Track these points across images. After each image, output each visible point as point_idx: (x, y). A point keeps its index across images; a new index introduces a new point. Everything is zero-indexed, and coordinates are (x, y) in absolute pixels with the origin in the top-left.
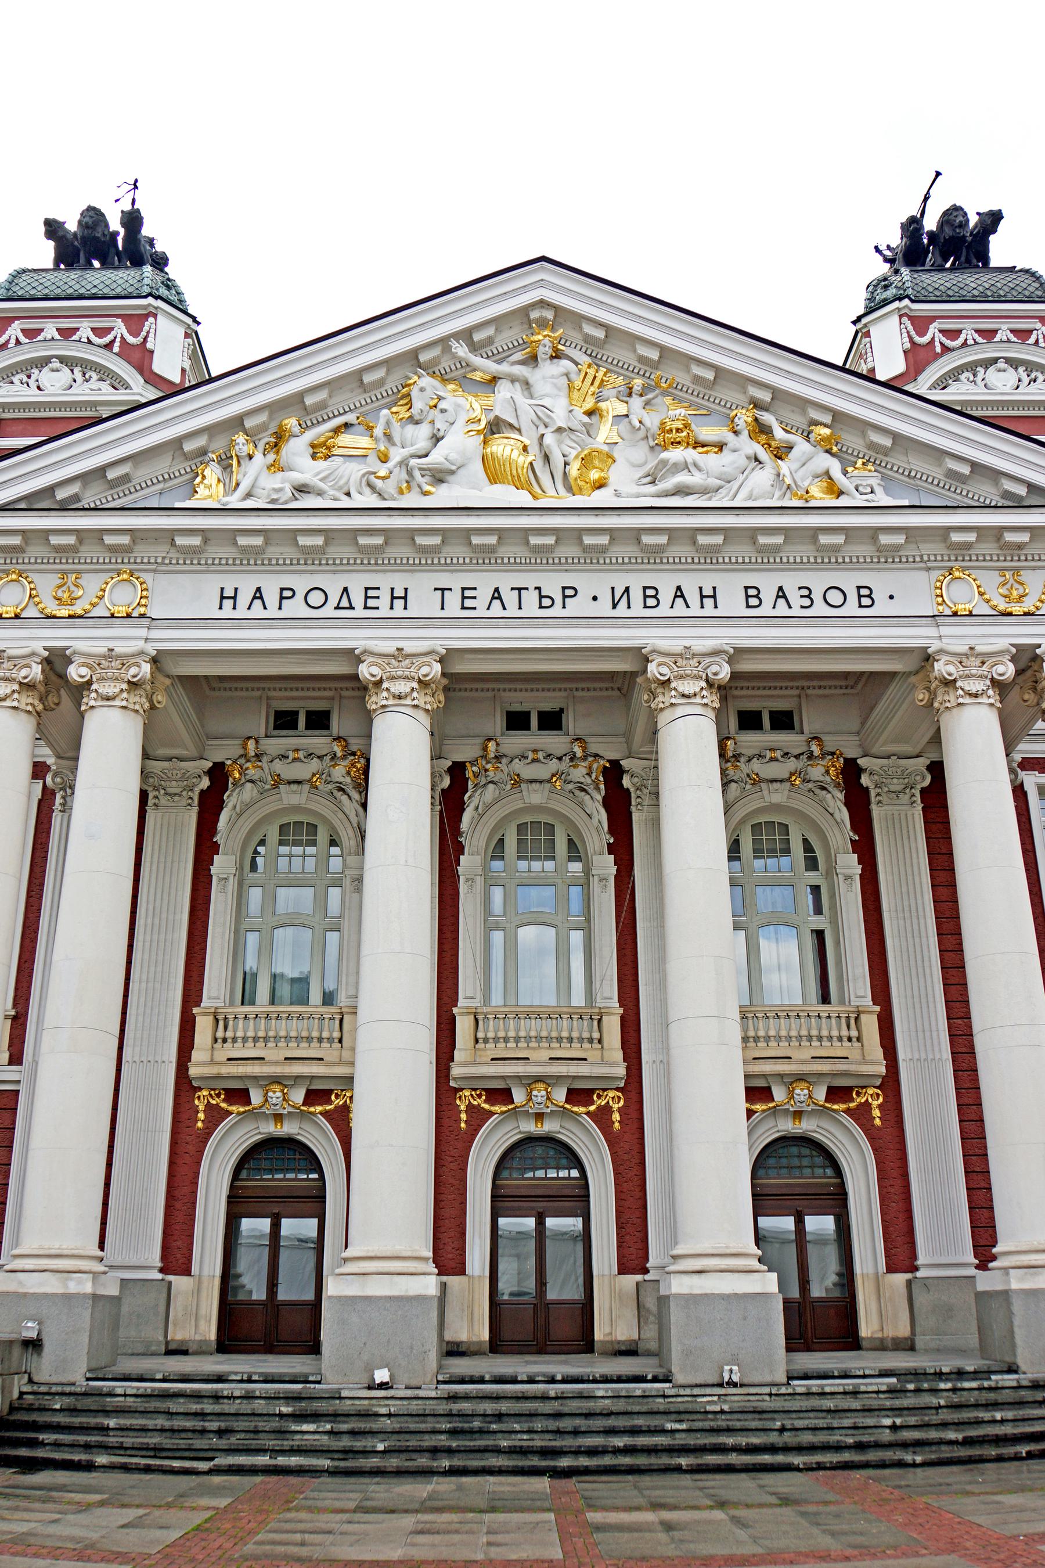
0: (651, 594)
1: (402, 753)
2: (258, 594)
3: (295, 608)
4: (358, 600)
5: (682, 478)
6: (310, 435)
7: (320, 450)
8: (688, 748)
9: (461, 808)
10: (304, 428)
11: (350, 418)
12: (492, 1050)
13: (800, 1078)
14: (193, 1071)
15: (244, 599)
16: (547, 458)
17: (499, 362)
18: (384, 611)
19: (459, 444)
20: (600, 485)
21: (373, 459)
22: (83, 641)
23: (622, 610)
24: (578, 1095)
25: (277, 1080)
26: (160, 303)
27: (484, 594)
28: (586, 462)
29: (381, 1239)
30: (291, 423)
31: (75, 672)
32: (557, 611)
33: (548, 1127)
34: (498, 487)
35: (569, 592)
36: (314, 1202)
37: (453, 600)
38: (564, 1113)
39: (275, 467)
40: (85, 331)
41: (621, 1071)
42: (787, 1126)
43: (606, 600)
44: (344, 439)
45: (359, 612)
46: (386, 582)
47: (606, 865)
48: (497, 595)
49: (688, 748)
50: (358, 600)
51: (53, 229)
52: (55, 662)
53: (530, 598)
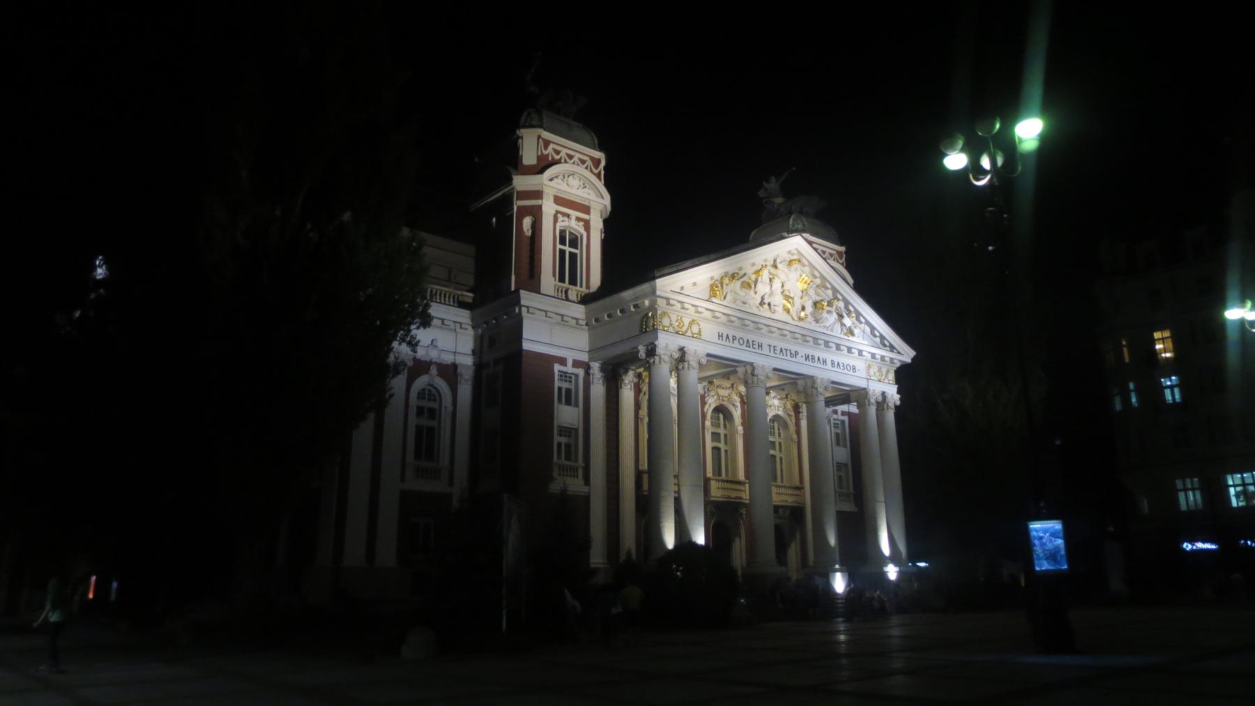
0: (813, 358)
3: (736, 344)
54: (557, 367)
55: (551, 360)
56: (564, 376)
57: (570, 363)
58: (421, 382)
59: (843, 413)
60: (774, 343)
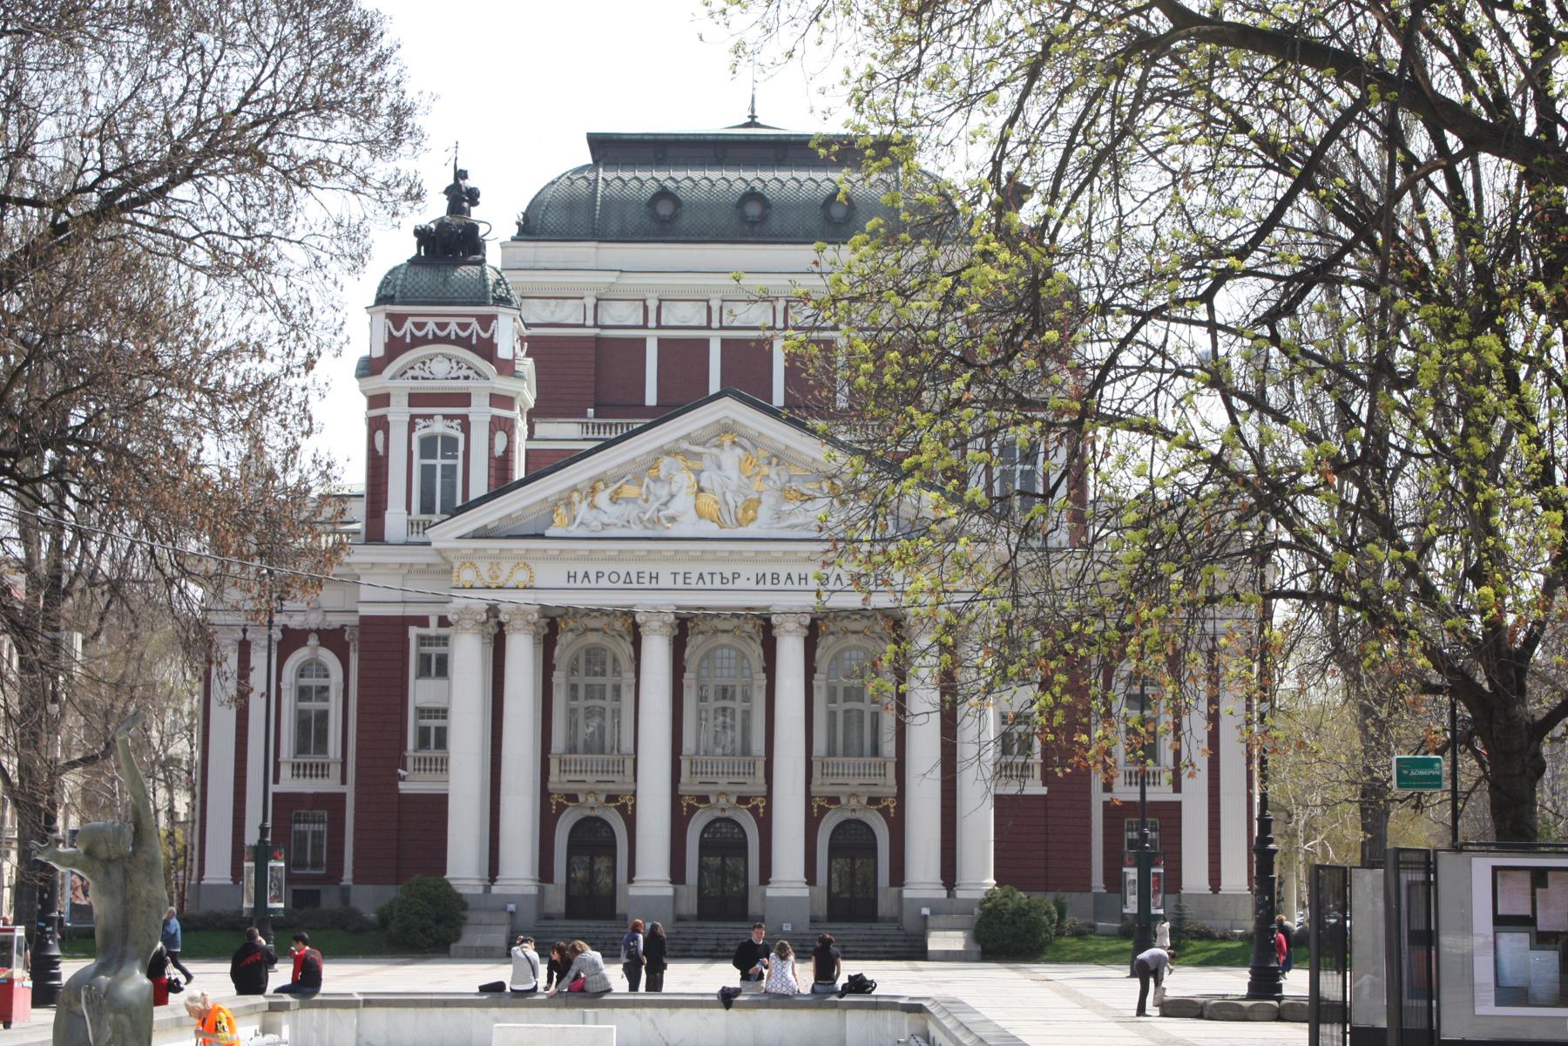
0: (775, 577)
1: (657, 652)
2: (586, 575)
3: (604, 582)
4: (634, 579)
5: (793, 521)
6: (609, 491)
7: (614, 499)
8: (790, 652)
9: (684, 646)
10: (606, 486)
11: (629, 477)
12: (699, 778)
13: (853, 795)
14: (550, 786)
15: (580, 576)
16: (727, 504)
17: (704, 444)
18: (647, 585)
20: (753, 520)
21: (640, 502)
23: (761, 586)
24: (743, 800)
25: (592, 792)
26: (501, 309)
27: (695, 576)
28: (745, 511)
29: (651, 874)
30: (601, 485)
31: (503, 618)
32: (730, 586)
33: (727, 814)
34: (702, 522)
35: (736, 576)
36: (610, 848)
37: (680, 579)
38: (735, 808)
39: (593, 506)
40: (453, 327)
41: (763, 788)
42: (848, 815)
43: (754, 580)
44: (626, 487)
45: (635, 585)
46: (648, 568)
47: (761, 679)
48: (701, 576)
49: (790, 652)
50: (634, 579)
51: (417, 233)
52: (493, 610)
53: (717, 578)
54: (414, 632)
55: (406, 621)
56: (423, 640)
57: (433, 621)
58: (299, 656)
60: (681, 569)
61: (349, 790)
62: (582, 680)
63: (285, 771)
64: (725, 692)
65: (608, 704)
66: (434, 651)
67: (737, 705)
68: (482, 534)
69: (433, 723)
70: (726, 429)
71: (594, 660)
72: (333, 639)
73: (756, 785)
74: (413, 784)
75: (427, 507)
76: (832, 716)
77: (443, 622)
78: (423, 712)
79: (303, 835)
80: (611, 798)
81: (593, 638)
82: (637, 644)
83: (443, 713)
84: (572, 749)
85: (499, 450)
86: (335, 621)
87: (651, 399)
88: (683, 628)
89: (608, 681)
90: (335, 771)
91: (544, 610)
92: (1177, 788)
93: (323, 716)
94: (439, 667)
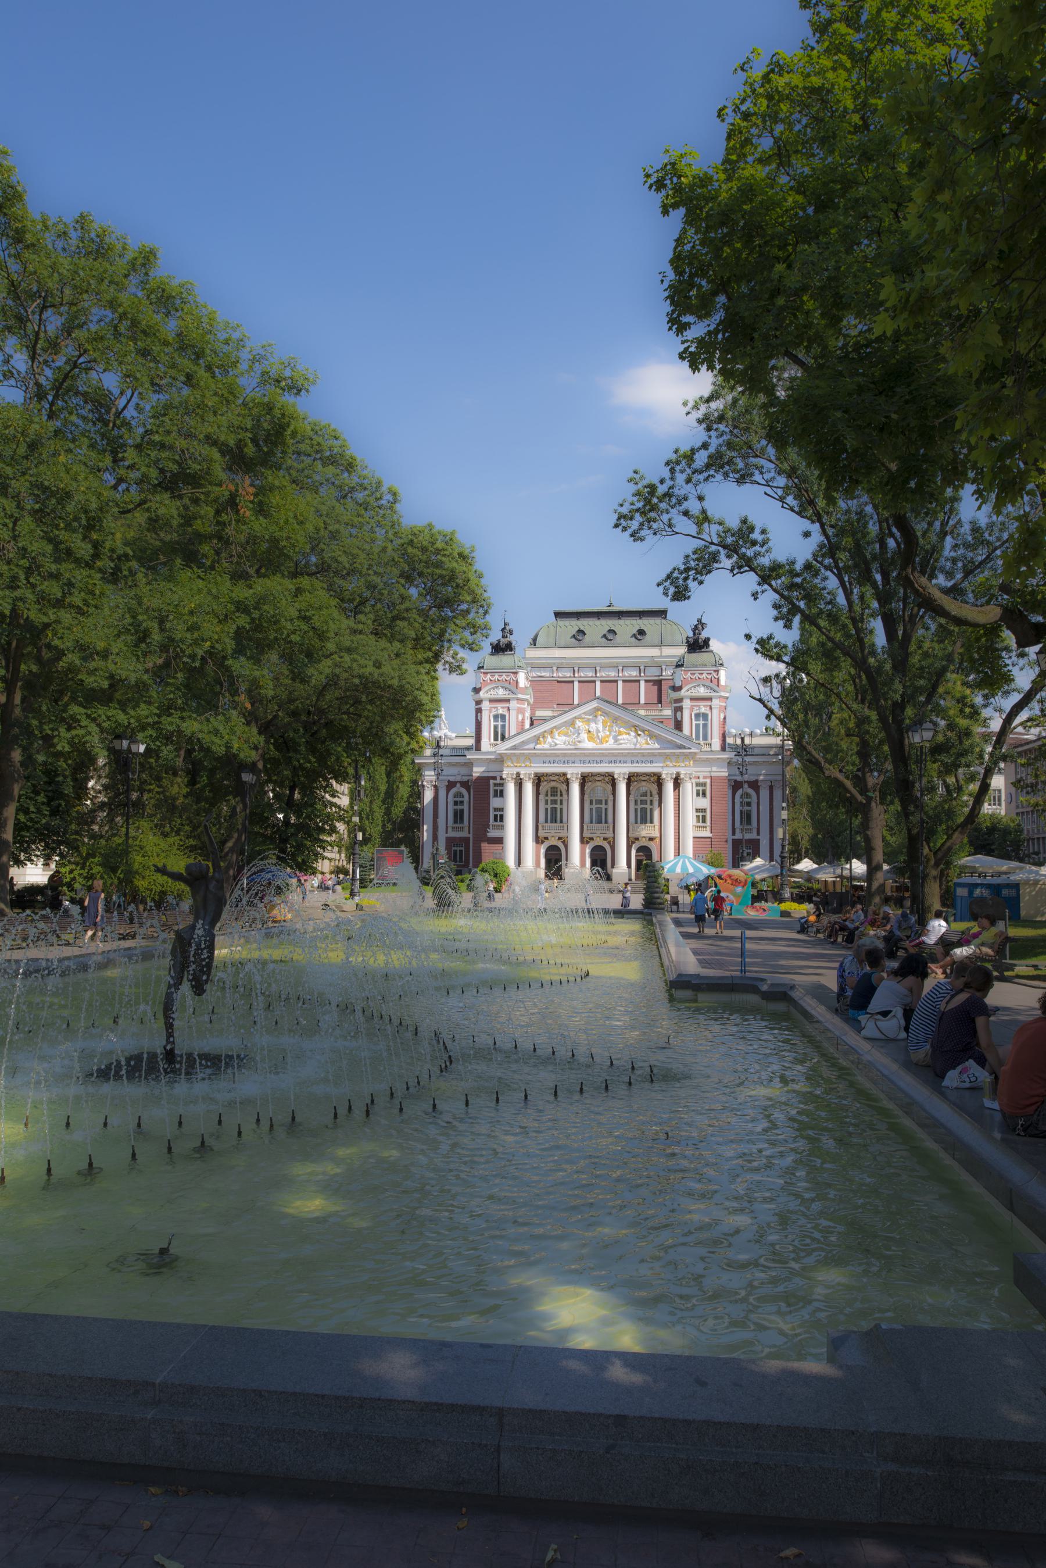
8: (622, 788)
19: (584, 736)
22: (523, 772)
24: (605, 839)
47: (611, 797)
49: (622, 788)
52: (518, 774)
54: (492, 782)
56: (495, 785)
58: (454, 791)
59: (705, 777)
61: (471, 836)
62: (549, 798)
63: (450, 829)
64: (599, 802)
65: (558, 806)
66: (499, 788)
67: (603, 806)
68: (514, 748)
69: (499, 813)
70: (597, 709)
71: (554, 791)
72: (465, 784)
73: (609, 834)
74: (492, 833)
75: (496, 739)
76: (636, 810)
77: (502, 778)
78: (496, 809)
79: (455, 852)
80: (560, 839)
81: (553, 784)
82: (568, 785)
83: (502, 810)
84: (546, 822)
85: (520, 717)
86: (465, 779)
87: (576, 702)
88: (584, 779)
89: (558, 798)
90: (466, 829)
91: (536, 774)
92: (758, 834)
93: (462, 811)
94: (501, 794)
